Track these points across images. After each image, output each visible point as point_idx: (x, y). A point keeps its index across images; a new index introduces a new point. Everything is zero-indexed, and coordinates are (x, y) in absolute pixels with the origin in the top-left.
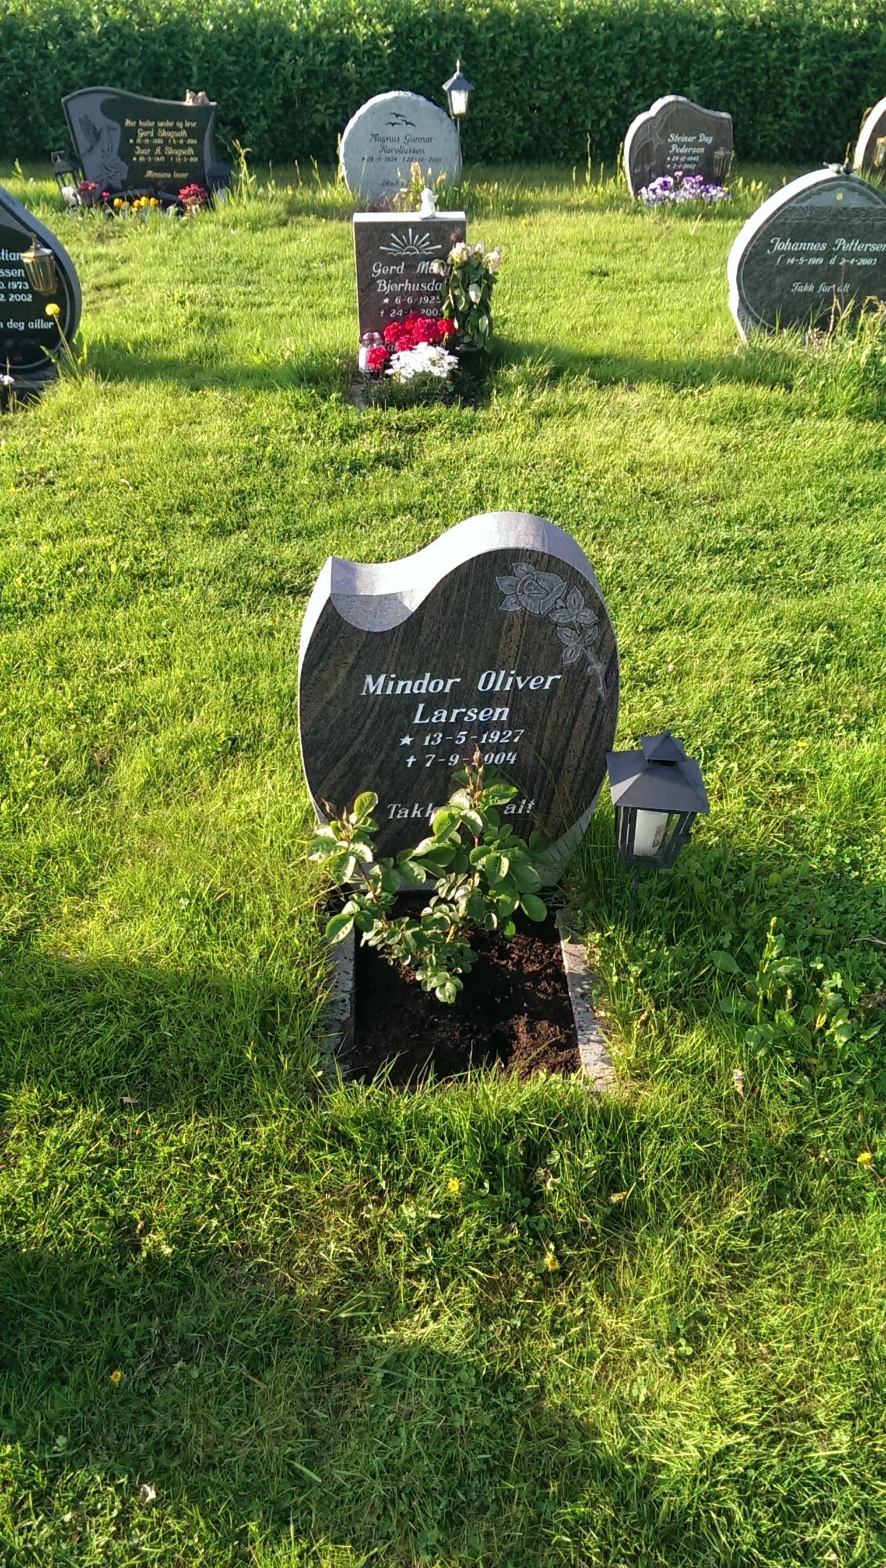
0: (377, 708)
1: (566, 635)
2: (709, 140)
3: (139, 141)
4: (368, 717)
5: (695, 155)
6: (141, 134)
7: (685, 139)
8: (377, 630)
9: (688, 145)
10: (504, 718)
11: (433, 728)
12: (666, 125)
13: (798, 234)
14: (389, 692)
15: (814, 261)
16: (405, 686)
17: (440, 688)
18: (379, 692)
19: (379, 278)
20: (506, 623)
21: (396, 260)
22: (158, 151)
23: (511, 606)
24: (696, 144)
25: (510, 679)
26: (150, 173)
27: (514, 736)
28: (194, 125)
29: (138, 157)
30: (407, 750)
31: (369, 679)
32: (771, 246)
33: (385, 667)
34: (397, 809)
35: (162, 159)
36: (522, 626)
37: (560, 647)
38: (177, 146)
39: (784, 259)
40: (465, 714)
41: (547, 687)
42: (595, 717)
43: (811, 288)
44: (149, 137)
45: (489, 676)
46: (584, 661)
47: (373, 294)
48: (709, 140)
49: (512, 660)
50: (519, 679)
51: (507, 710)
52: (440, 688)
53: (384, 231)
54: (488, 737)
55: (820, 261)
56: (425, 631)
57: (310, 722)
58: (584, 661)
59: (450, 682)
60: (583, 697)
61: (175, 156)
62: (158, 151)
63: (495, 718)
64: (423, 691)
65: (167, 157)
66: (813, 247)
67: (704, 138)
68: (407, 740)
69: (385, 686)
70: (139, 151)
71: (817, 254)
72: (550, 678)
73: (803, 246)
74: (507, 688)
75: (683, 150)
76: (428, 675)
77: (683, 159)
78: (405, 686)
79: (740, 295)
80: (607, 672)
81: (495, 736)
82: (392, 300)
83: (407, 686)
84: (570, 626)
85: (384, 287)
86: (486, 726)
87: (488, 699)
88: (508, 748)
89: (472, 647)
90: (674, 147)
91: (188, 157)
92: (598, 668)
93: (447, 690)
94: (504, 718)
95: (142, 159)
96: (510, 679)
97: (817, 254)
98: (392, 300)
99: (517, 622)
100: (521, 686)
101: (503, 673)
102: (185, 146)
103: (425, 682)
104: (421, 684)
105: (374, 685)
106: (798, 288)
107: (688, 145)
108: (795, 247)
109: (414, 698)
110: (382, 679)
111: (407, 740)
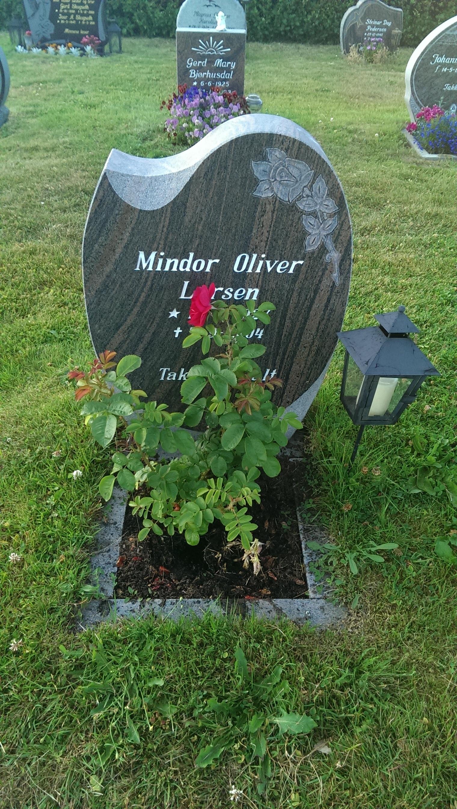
0: (149, 283)
1: (308, 222)
2: (389, 24)
3: (61, 11)
4: (142, 291)
6: (62, 7)
7: (375, 23)
8: (148, 208)
9: (377, 26)
10: (255, 298)
12: (365, 13)
14: (159, 269)
16: (172, 264)
17: (202, 268)
18: (150, 268)
19: (190, 69)
21: (202, 58)
22: (72, 17)
23: (264, 192)
24: (381, 26)
25: (261, 262)
26: (67, 31)
28: (93, 2)
29: (60, 20)
30: (175, 322)
31: (142, 255)
32: (433, 60)
33: (155, 245)
35: (74, 22)
36: (273, 212)
37: (305, 234)
38: (83, 15)
40: (222, 293)
41: (291, 271)
42: (329, 300)
44: (67, 9)
45: (243, 259)
46: (323, 249)
47: (187, 79)
48: (389, 24)
49: (263, 244)
50: (268, 262)
51: (257, 291)
52: (202, 268)
57: (93, 293)
58: (323, 249)
59: (211, 262)
60: (320, 282)
61: (81, 21)
62: (72, 17)
64: (188, 269)
65: (77, 21)
68: (174, 314)
70: (61, 17)
72: (294, 263)
74: (258, 270)
75: (374, 29)
76: (192, 255)
77: (374, 35)
78: (172, 264)
79: (412, 90)
80: (342, 260)
82: (199, 83)
83: (174, 265)
84: (314, 214)
85: (193, 74)
87: (242, 280)
89: (229, 230)
90: (369, 27)
91: (89, 21)
92: (334, 256)
93: (208, 270)
94: (255, 298)
95: (62, 22)
96: (261, 262)
98: (199, 83)
99: (269, 208)
100: (269, 269)
101: (255, 256)
102: (88, 15)
103: (189, 261)
104: (186, 263)
105: (146, 261)
107: (377, 26)
108: (448, 61)
109: (180, 276)
110: (152, 256)
111: (174, 314)
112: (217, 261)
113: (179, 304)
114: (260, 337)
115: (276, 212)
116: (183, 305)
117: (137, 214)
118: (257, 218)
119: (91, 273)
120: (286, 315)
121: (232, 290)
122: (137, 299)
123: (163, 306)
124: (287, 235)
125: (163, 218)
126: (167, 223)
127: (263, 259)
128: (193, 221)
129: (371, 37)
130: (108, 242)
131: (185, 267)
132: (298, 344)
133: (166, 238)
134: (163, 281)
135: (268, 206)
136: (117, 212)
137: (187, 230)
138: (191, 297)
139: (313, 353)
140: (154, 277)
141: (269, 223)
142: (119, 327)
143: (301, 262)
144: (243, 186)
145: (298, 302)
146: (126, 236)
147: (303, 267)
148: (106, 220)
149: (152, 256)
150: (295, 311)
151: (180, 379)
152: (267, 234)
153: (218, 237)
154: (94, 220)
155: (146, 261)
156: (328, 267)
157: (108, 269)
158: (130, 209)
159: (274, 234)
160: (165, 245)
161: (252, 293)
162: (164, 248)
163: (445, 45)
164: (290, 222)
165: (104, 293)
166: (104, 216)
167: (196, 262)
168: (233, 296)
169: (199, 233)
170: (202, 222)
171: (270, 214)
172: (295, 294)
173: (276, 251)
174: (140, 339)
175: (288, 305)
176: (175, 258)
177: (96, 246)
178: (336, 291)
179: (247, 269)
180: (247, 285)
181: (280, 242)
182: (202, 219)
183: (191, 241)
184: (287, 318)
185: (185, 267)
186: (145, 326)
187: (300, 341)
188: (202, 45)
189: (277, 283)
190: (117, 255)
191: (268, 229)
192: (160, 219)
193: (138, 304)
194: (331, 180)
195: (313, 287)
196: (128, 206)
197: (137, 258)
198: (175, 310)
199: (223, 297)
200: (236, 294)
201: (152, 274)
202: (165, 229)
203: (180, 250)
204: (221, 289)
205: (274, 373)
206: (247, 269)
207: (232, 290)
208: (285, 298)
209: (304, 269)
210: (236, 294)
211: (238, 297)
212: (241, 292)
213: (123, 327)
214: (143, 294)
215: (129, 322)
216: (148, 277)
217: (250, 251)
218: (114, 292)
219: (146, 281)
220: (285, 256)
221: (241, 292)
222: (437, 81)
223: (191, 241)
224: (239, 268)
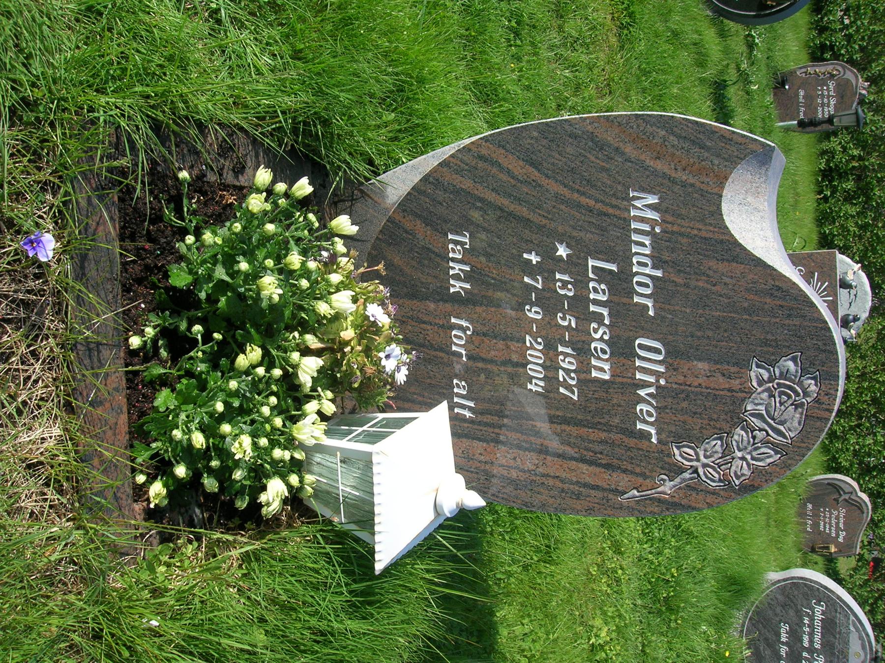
0: (611, 211)
2: (841, 540)
5: (830, 529)
8: (725, 207)
9: (837, 524)
11: (581, 282)
13: (829, 625)
15: (806, 638)
16: (643, 245)
17: (639, 289)
20: (733, 369)
24: (838, 528)
25: (652, 379)
27: (569, 387)
30: (548, 254)
31: (652, 200)
32: (818, 603)
33: (670, 218)
34: (462, 244)
36: (730, 390)
37: (697, 440)
39: (808, 615)
40: (601, 323)
41: (640, 426)
42: (596, 487)
43: (784, 639)
45: (657, 351)
46: (676, 470)
48: (841, 540)
50: (652, 390)
52: (639, 289)
53: (830, 276)
54: (566, 355)
55: (806, 644)
56: (722, 267)
60: (625, 471)
63: (594, 362)
66: (817, 638)
67: (842, 534)
68: (562, 251)
69: (642, 220)
71: (811, 641)
72: (653, 432)
73: (818, 630)
74: (639, 376)
75: (833, 522)
76: (659, 273)
78: (643, 245)
79: (779, 581)
80: (659, 500)
81: (568, 363)
83: (642, 249)
84: (727, 451)
86: (582, 351)
87: (622, 350)
88: (551, 380)
90: (836, 513)
93: (636, 299)
94: (594, 374)
96: (652, 379)
97: (811, 641)
99: (735, 383)
100: (642, 393)
101: (662, 369)
103: (647, 271)
104: (646, 265)
105: (644, 206)
106: (784, 629)
107: (837, 524)
108: (817, 623)
109: (625, 260)
110: (651, 215)
111: (562, 251)
112: (651, 313)
113: (578, 258)
114: (529, 386)
115: (729, 394)
116: (577, 265)
117: (715, 190)
118: (718, 366)
119: (620, 125)
120: (569, 424)
121: (606, 337)
122: (583, 194)
123: (575, 234)
124: (695, 413)
125: (711, 228)
126: (704, 234)
127: (658, 381)
128: (711, 273)
129: (825, 517)
130: (671, 150)
131: (639, 263)
132: (519, 447)
133: (682, 234)
134: (615, 233)
135: (738, 381)
136: (716, 162)
137: (696, 265)
138: (591, 275)
139: (505, 473)
140: (620, 218)
141: (712, 385)
142: (536, 168)
143: (654, 440)
144: (766, 343)
145: (590, 441)
146: (683, 176)
147: (647, 443)
148: (702, 147)
149: (651, 215)
150: (576, 437)
151: (451, 264)
152: (696, 384)
153: (688, 311)
154: (702, 129)
155: (645, 206)
156: (648, 481)
157: (628, 149)
158: (722, 180)
159: (697, 394)
160: (673, 233)
161: (602, 370)
162: (666, 232)
163: (835, 617)
164: (715, 416)
165: (590, 144)
166: (708, 144)
167: (647, 281)
168: (597, 340)
169: (693, 283)
170: (709, 286)
171: (727, 386)
172: (603, 435)
173: (670, 400)
174: (519, 200)
175: (585, 426)
176: (653, 248)
177: (663, 133)
178: (611, 496)
179: (640, 357)
180: (615, 359)
181: (685, 404)
182: (714, 285)
183: (679, 271)
184: (564, 427)
185: (639, 263)
186: (539, 207)
187: (526, 449)
188: (821, 286)
189: (620, 406)
190: (652, 163)
191: (704, 384)
192: (711, 224)
193: (576, 195)
194: (778, 470)
195: (615, 462)
196: (726, 179)
197: (649, 192)
198: (569, 252)
199: (594, 325)
200: (600, 345)
201: (626, 215)
202: (696, 232)
203: (666, 256)
204: (607, 322)
205: (468, 414)
206: (640, 357)
207: (606, 337)
208: (597, 420)
209: (644, 444)
210: (600, 345)
211: (596, 349)
212: (604, 352)
213: (536, 173)
214: (591, 203)
215: (544, 181)
216: (620, 209)
217: (669, 360)
218: (593, 158)
219: (613, 206)
220: (663, 415)
221: (604, 352)
222: (792, 613)
223: (679, 271)
224: (641, 346)
